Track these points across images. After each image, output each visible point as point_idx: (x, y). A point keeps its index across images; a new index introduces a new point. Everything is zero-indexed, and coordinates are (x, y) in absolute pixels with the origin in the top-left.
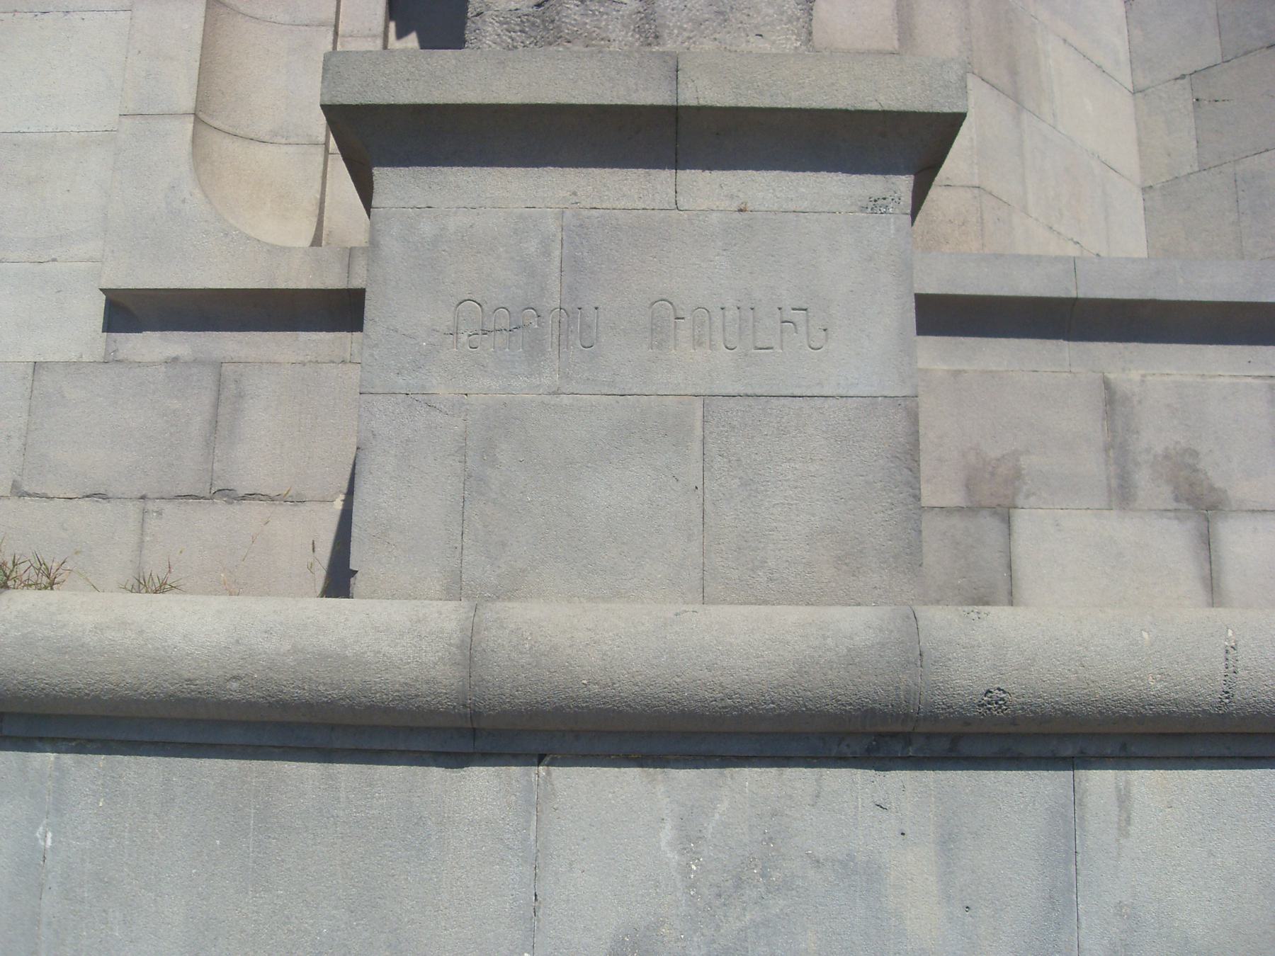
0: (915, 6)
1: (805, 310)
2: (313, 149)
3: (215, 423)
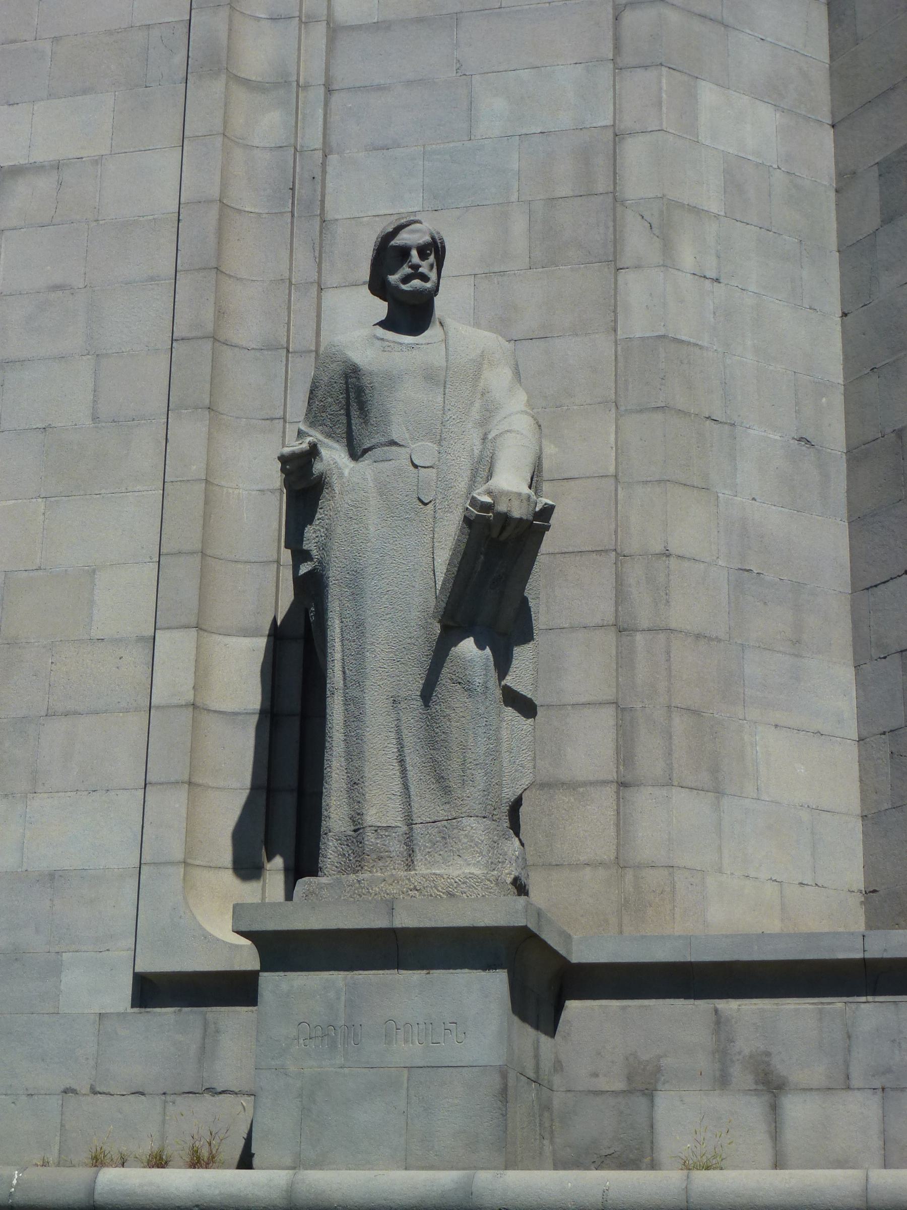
0: (636, 740)
1: (456, 1023)
3: (203, 1048)
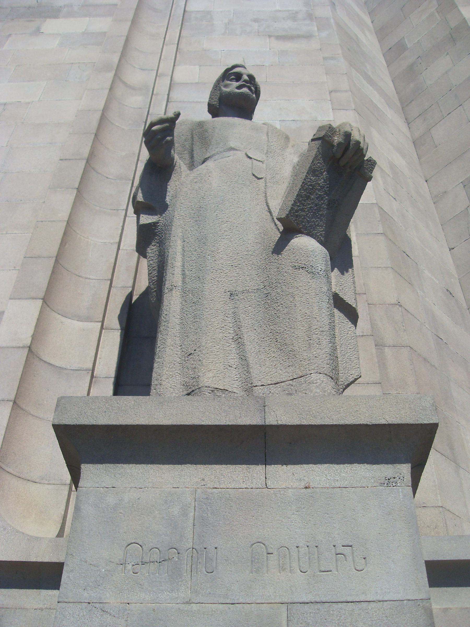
1: (351, 546)
2: (63, 487)
